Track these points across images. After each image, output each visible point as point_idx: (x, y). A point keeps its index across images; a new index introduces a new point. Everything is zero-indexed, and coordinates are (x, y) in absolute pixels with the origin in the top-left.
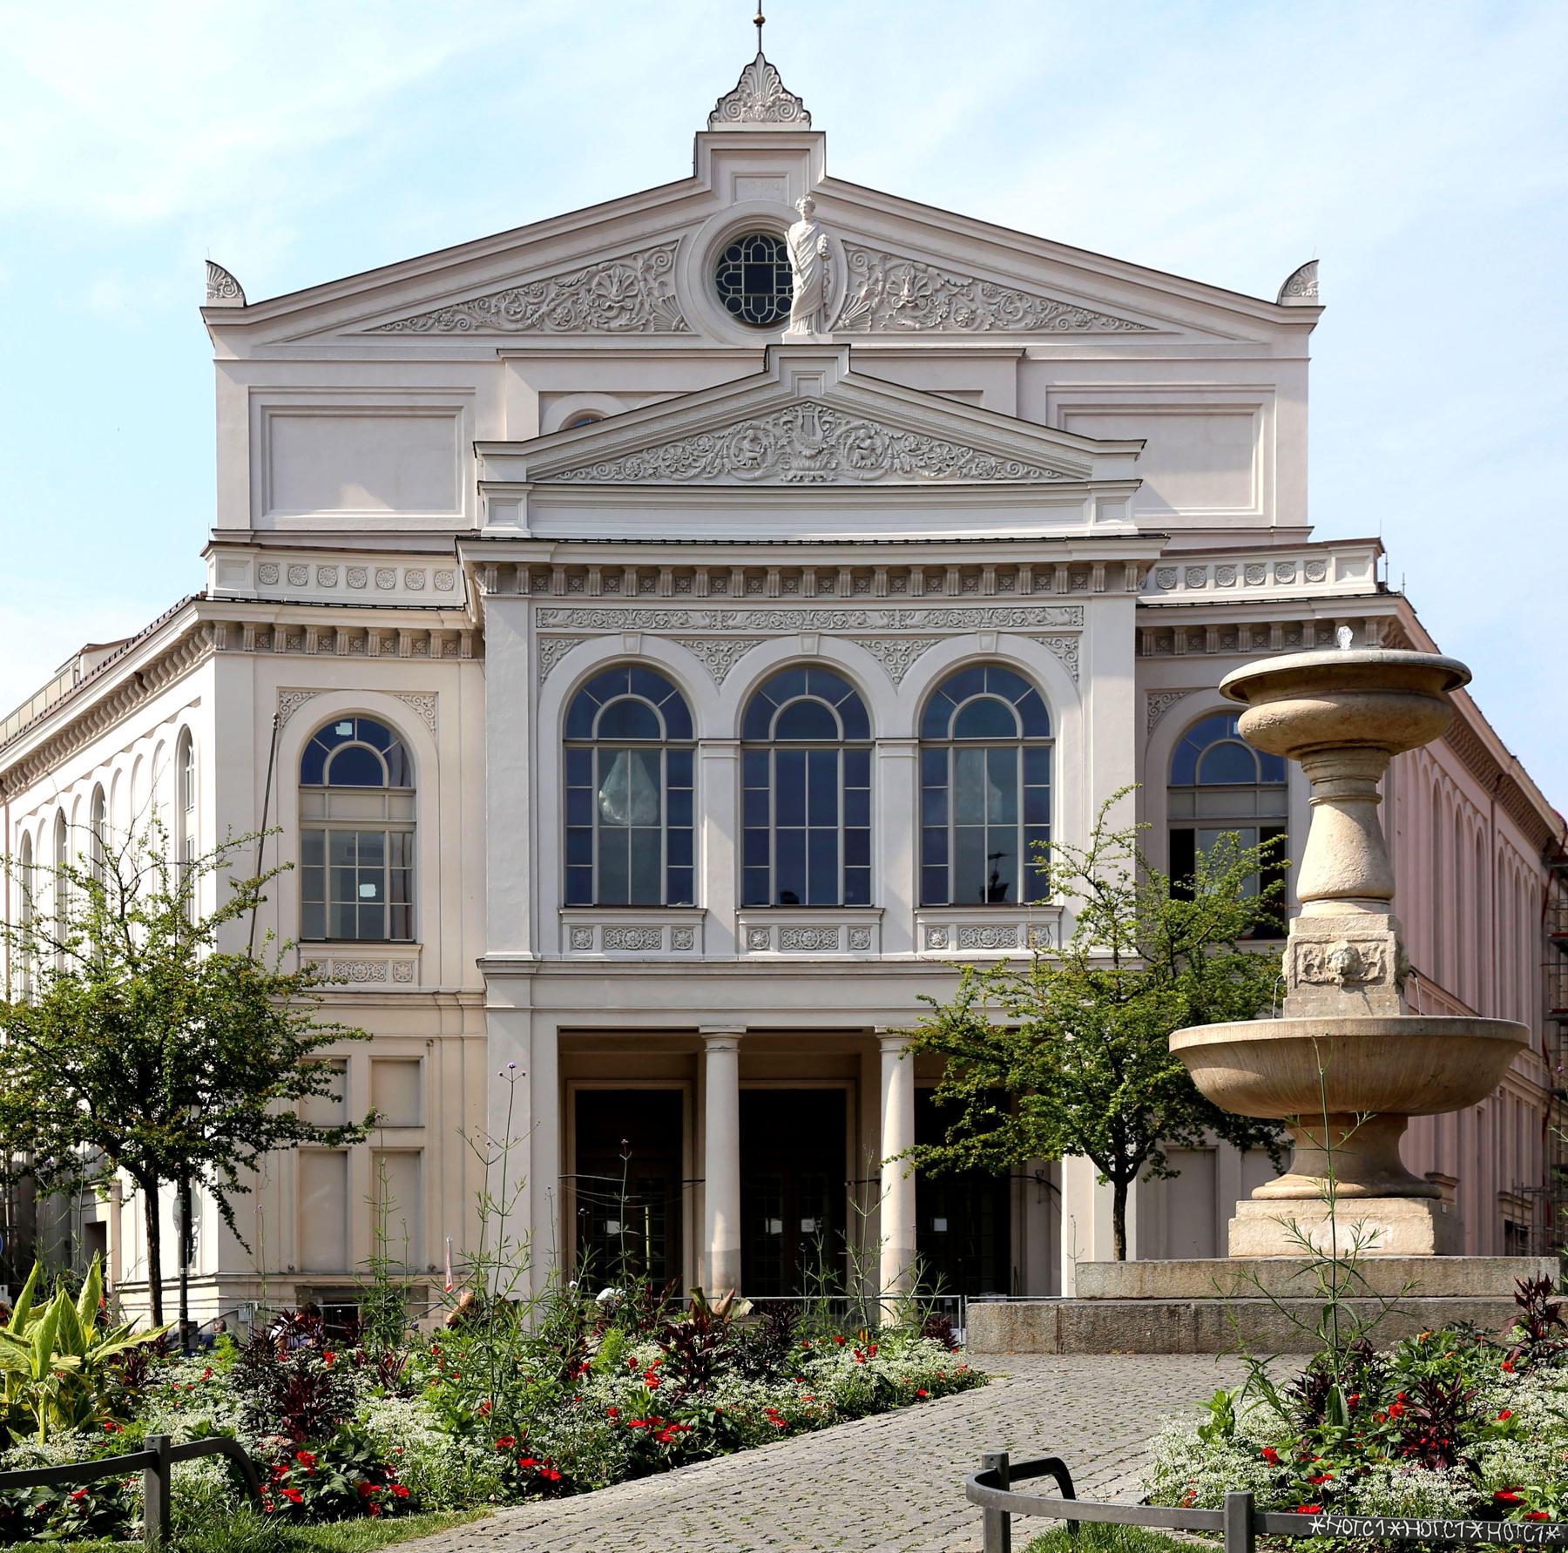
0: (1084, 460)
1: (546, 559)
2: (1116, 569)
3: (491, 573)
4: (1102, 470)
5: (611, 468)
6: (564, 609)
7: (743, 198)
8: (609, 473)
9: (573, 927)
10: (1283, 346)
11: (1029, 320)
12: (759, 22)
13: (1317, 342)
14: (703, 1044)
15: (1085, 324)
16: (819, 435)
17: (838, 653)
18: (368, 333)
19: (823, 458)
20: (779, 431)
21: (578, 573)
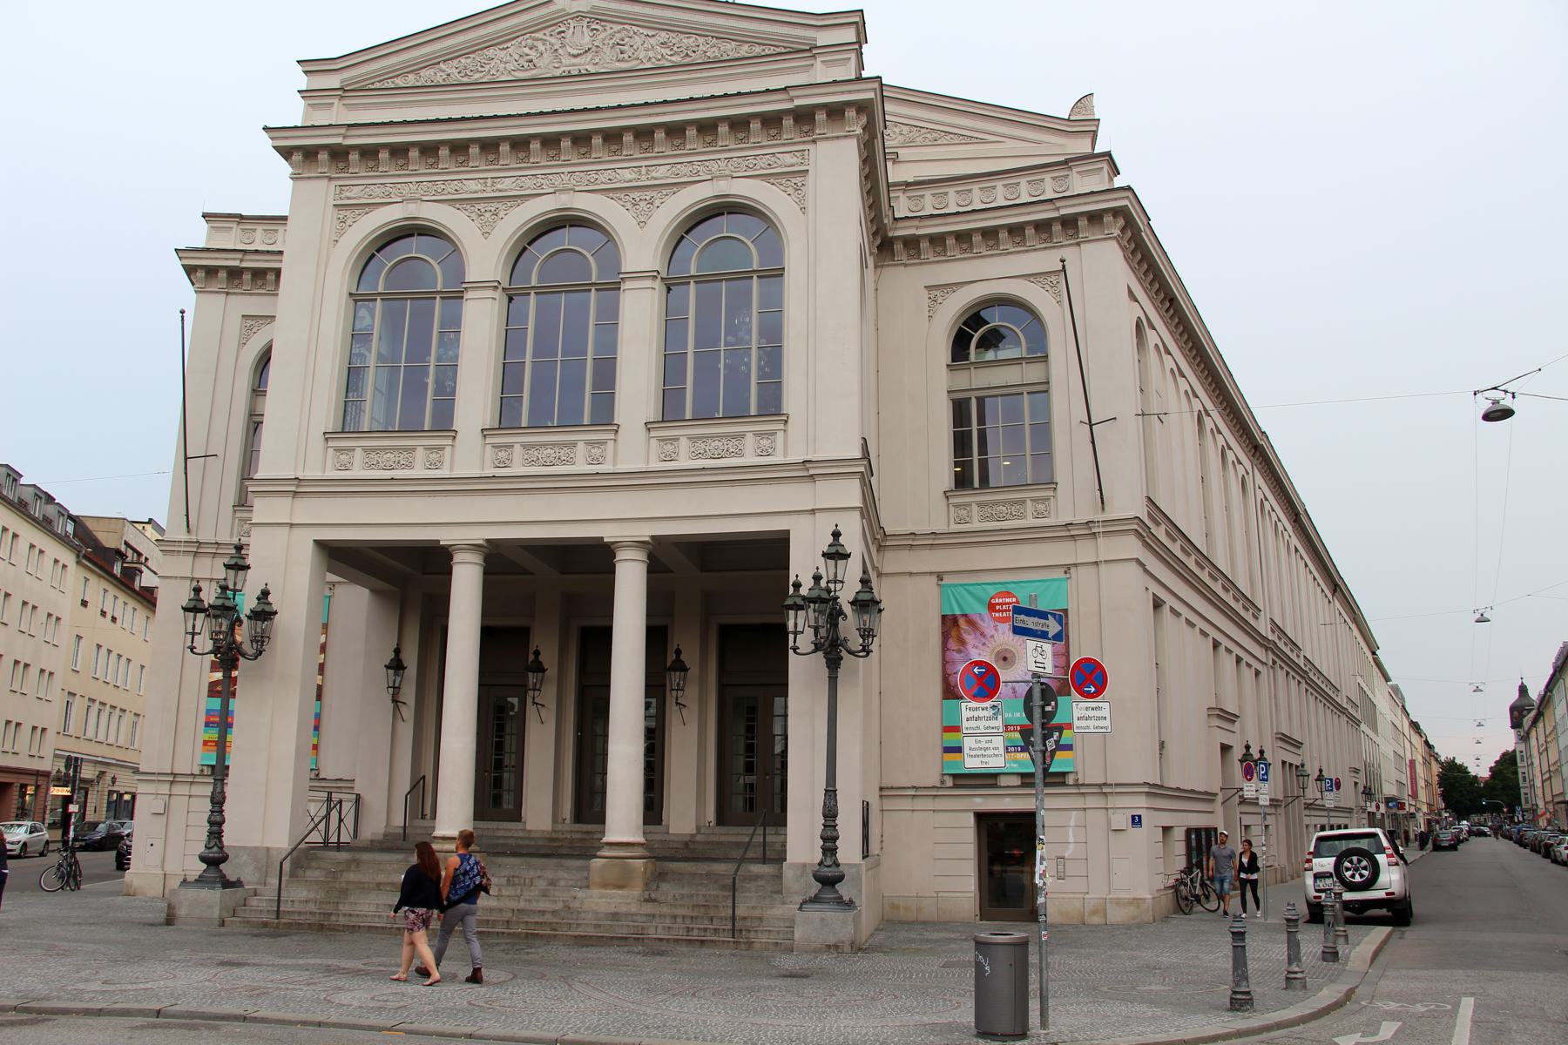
0: (810, 33)
2: (835, 112)
3: (297, 157)
4: (823, 38)
5: (411, 77)
6: (360, 184)
8: (411, 80)
9: (337, 450)
11: (901, 138)
14: (451, 558)
15: (939, 137)
16: (587, 39)
17: (584, 203)
19: (590, 55)
20: (553, 40)
21: (369, 153)
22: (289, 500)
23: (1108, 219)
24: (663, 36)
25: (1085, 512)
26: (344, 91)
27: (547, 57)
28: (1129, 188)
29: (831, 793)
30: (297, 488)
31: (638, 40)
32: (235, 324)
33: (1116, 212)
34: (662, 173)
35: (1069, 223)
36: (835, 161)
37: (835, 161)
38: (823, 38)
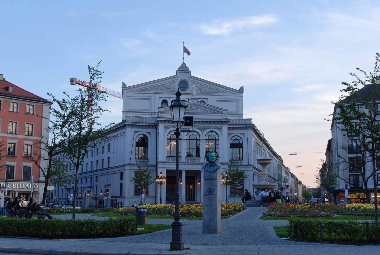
0: (222, 111)
1: (166, 120)
6: (168, 125)
7: (182, 77)
10: (240, 95)
12: (183, 59)
13: (244, 94)
18: (140, 90)
22: (163, 165)
23: (251, 127)
24: (204, 108)
25: (247, 164)
26: (164, 112)
27: (190, 109)
28: (254, 124)
29: (227, 197)
30: (164, 163)
31: (201, 108)
32: (133, 133)
33: (252, 127)
34: (205, 127)
35: (246, 127)
36: (225, 127)
37: (225, 127)
38: (224, 112)
